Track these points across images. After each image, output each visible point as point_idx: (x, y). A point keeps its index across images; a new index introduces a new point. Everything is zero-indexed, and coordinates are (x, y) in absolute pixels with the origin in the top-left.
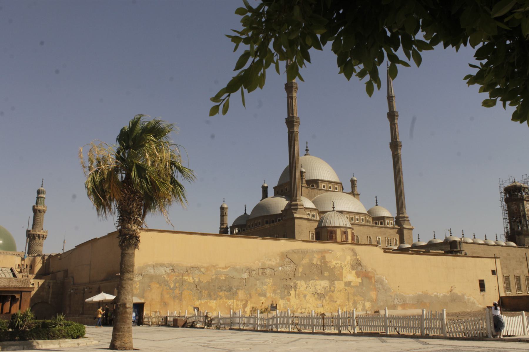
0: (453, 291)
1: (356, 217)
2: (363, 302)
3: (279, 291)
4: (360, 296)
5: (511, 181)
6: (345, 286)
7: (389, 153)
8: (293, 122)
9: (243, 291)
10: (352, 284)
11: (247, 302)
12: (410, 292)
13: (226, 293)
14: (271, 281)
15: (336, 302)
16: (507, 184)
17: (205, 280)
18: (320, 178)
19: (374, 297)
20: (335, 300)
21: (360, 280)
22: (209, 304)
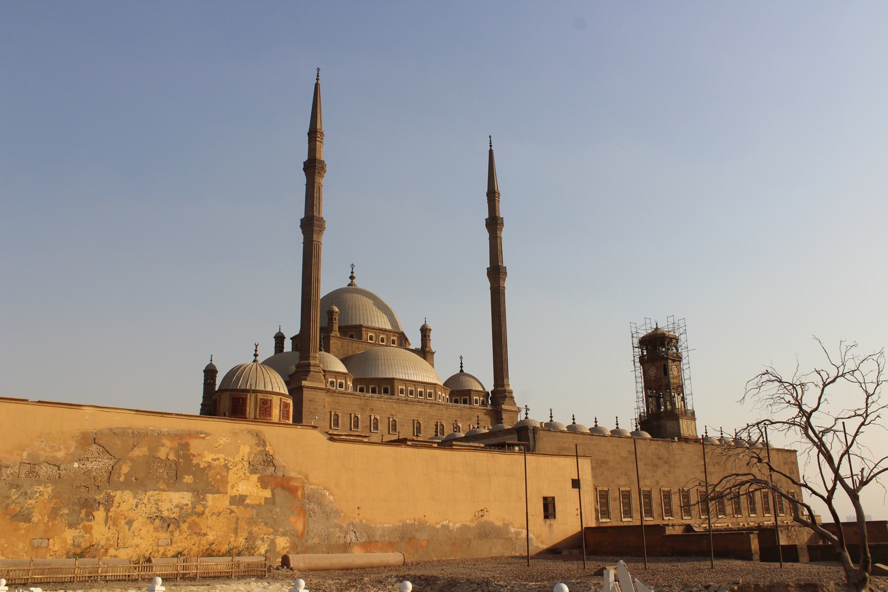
0: (485, 518)
1: (419, 390)
2: (272, 537)
3: (66, 511)
4: (266, 524)
5: (648, 327)
6: (231, 504)
7: (486, 284)
10: (248, 501)
12: (384, 518)
14: (49, 490)
15: (205, 534)
16: (642, 334)
18: (365, 324)
19: (300, 527)
20: (203, 531)
21: (267, 493)
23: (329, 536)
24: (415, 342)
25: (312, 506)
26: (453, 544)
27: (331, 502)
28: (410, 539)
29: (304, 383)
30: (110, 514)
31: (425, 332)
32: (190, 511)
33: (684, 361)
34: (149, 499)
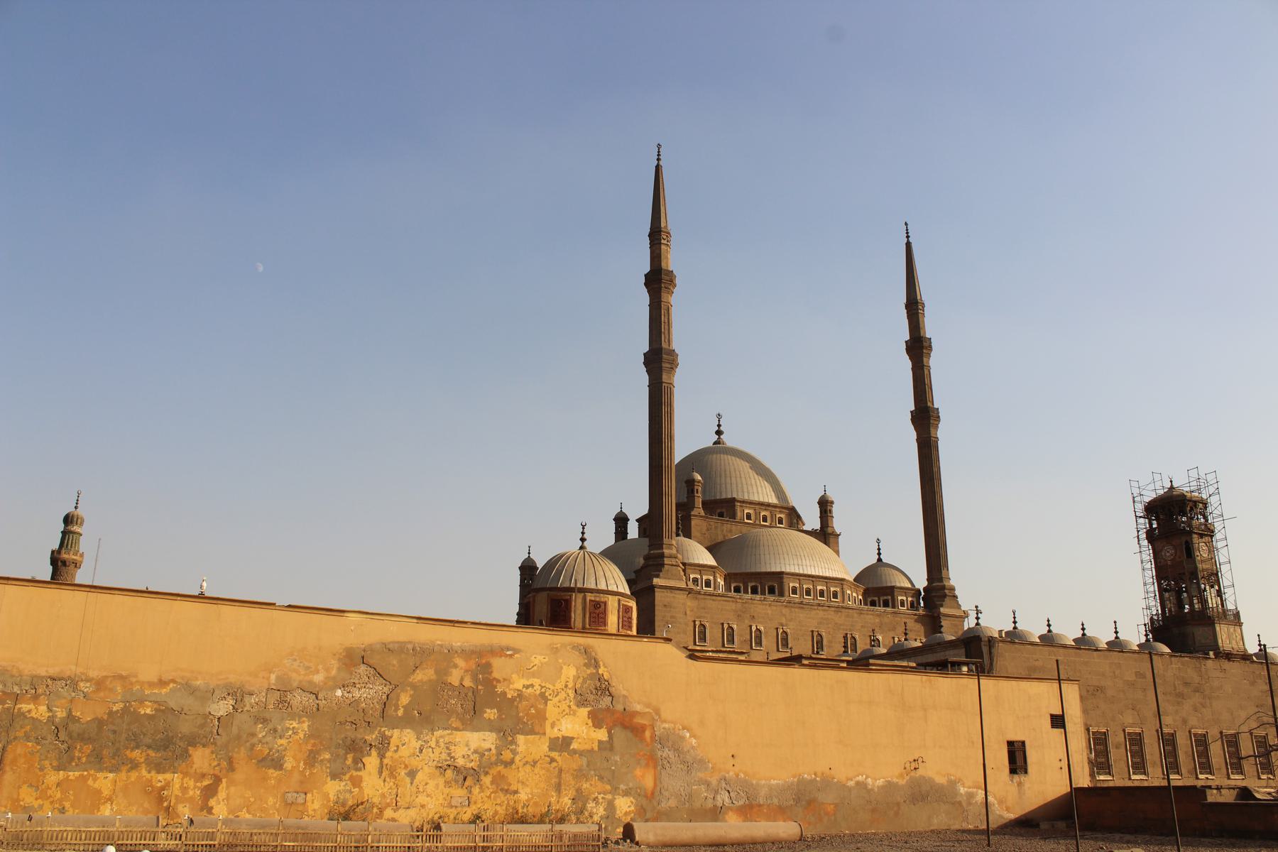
0: (919, 772)
1: (819, 588)
2: (609, 797)
3: (327, 756)
4: (601, 778)
5: (1158, 485)
6: (551, 749)
7: (910, 435)
8: (660, 360)
9: (207, 751)
10: (574, 746)
11: (218, 780)
12: (772, 771)
13: (151, 752)
14: (305, 726)
15: (516, 792)
16: (1149, 496)
17: (86, 714)
18: (740, 497)
19: (649, 782)
20: (513, 788)
21: (602, 735)
22: (90, 782)
23: (691, 796)
24: (812, 520)
25: (666, 752)
26: (874, 811)
27: (693, 747)
28: (810, 803)
29: (656, 581)
30: (386, 761)
31: (825, 505)
32: (494, 759)
33: (1218, 536)
34: (437, 742)
